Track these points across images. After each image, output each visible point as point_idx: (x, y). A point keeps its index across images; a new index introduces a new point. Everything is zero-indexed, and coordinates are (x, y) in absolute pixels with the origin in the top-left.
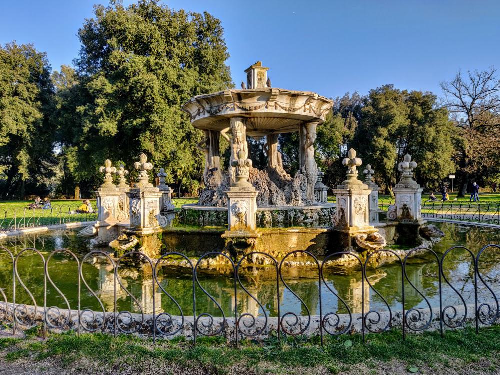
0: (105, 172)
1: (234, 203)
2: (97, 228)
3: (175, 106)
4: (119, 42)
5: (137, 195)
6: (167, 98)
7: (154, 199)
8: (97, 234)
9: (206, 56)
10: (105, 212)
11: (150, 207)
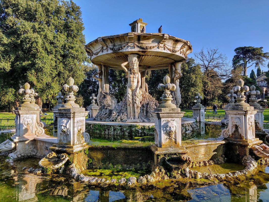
0: (25, 93)
1: (164, 122)
2: (15, 143)
3: (51, 55)
4: (13, 11)
5: (68, 115)
6: (46, 49)
7: (82, 118)
8: (15, 148)
9: (72, 26)
10: (24, 128)
11: (79, 126)
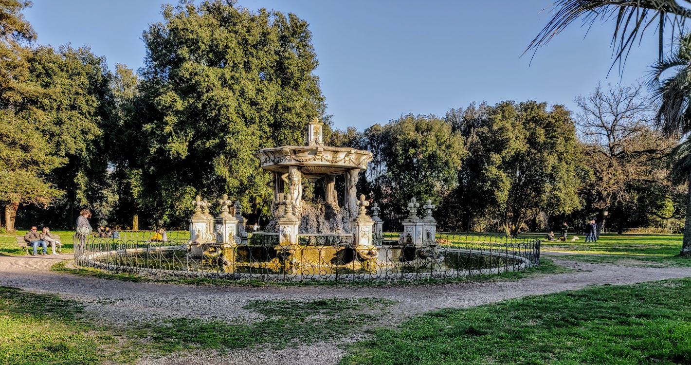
1: (282, 228)
2: (190, 246)
3: (252, 126)
4: (191, 52)
6: (244, 116)
9: (290, 66)
10: (196, 234)
